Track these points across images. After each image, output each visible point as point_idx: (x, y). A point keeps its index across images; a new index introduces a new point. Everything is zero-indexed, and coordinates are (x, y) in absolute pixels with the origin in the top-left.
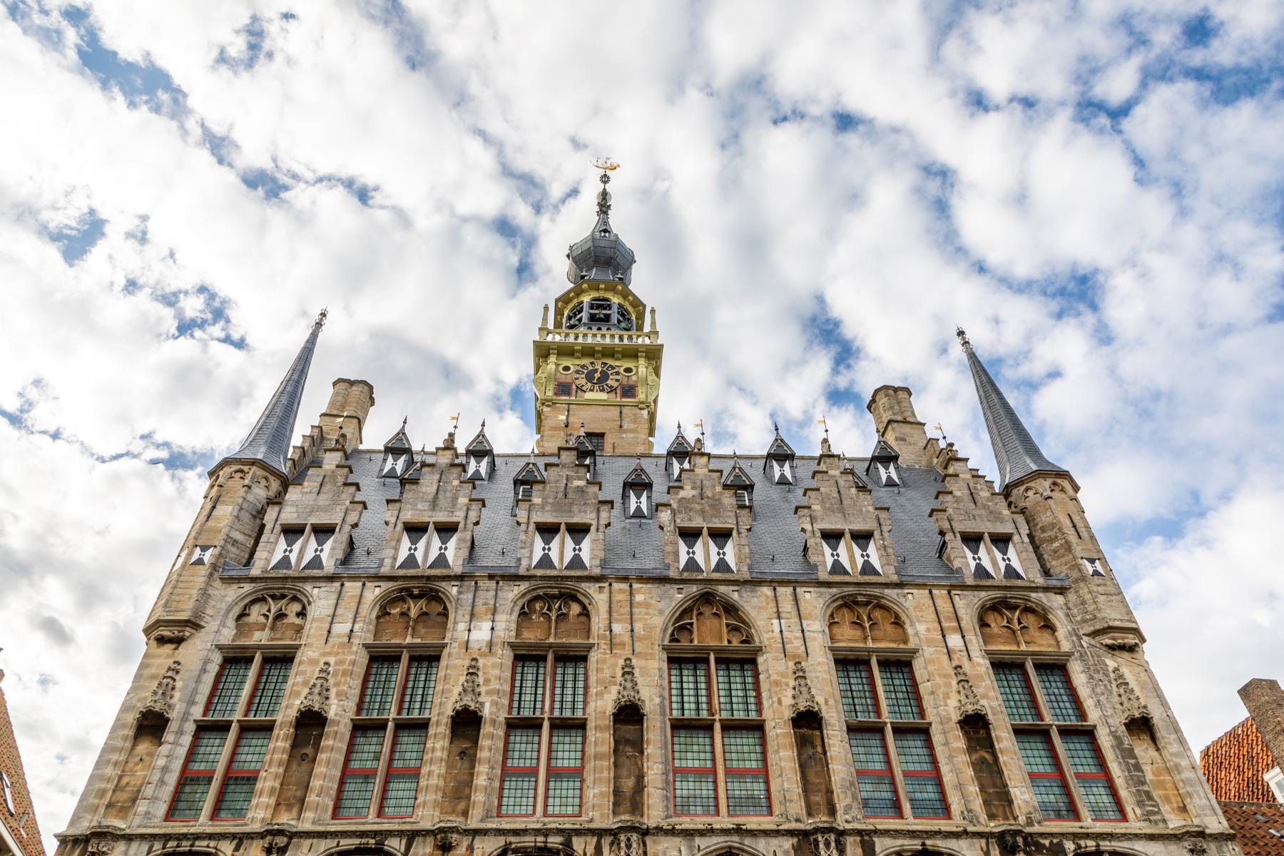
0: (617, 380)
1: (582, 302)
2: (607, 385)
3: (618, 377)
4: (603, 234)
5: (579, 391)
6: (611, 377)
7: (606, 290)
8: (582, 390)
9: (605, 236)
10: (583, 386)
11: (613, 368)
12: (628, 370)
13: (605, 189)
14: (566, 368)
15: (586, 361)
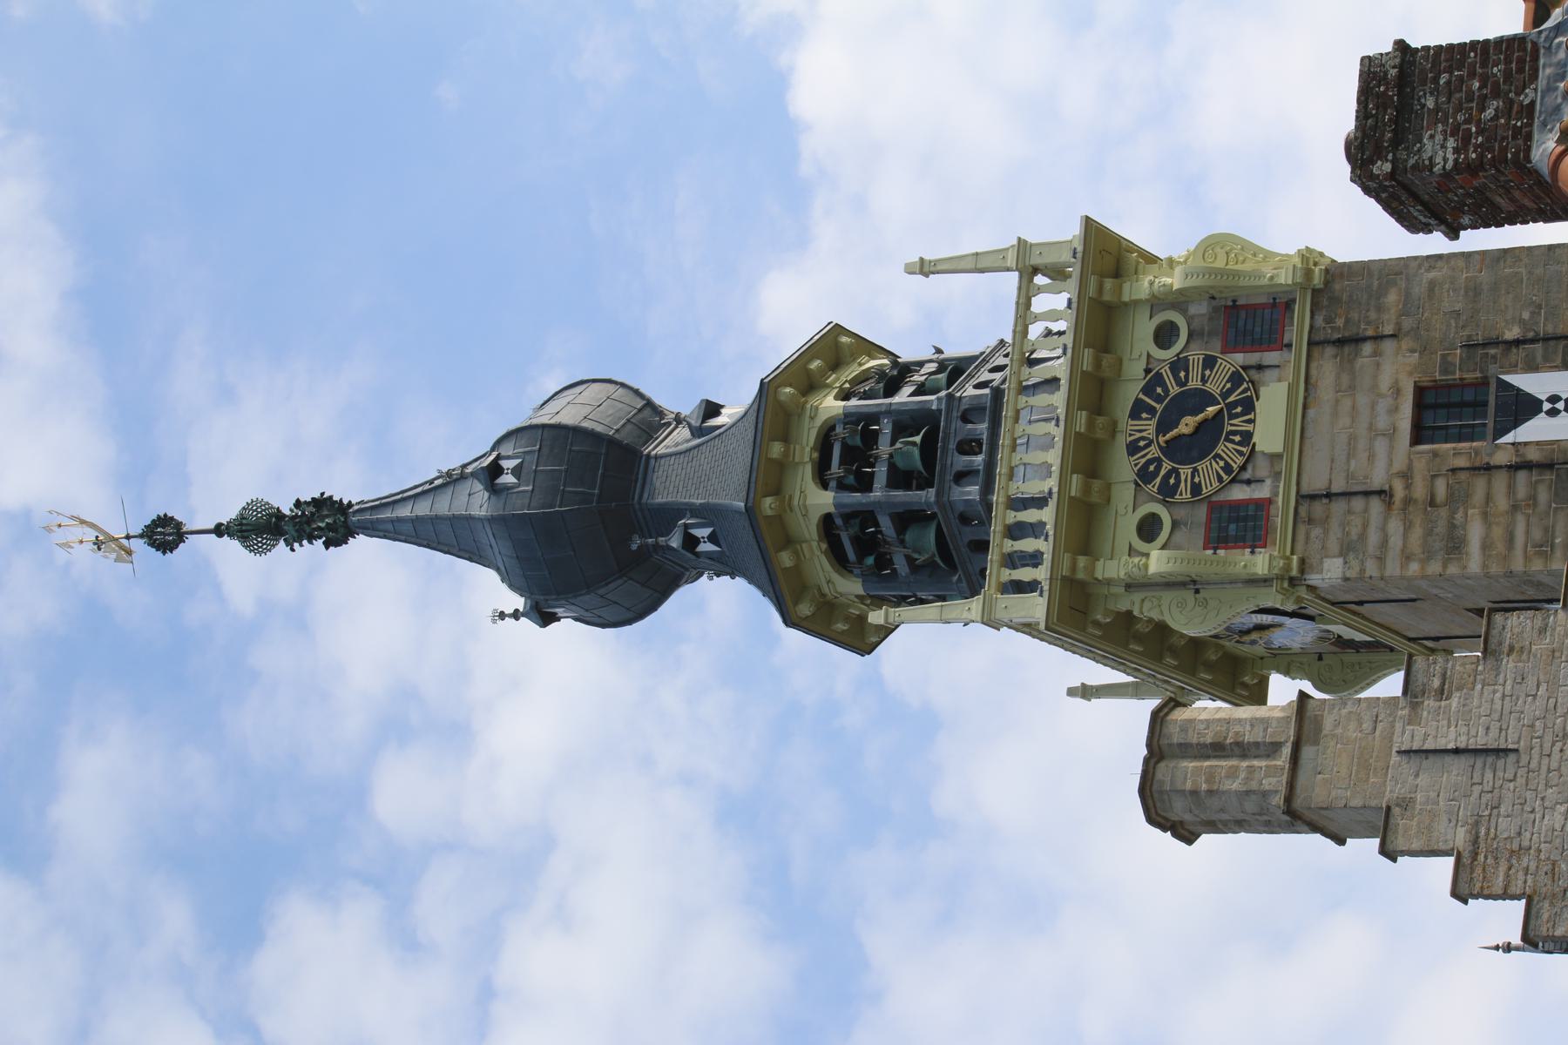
0: (1209, 362)
1: (827, 520)
2: (1225, 395)
3: (1196, 356)
4: (508, 479)
5: (1246, 475)
6: (1195, 383)
7: (786, 438)
8: (1243, 468)
9: (517, 471)
10: (1227, 468)
11: (1153, 383)
12: (1165, 335)
13: (219, 531)
14: (1149, 528)
15: (1123, 469)
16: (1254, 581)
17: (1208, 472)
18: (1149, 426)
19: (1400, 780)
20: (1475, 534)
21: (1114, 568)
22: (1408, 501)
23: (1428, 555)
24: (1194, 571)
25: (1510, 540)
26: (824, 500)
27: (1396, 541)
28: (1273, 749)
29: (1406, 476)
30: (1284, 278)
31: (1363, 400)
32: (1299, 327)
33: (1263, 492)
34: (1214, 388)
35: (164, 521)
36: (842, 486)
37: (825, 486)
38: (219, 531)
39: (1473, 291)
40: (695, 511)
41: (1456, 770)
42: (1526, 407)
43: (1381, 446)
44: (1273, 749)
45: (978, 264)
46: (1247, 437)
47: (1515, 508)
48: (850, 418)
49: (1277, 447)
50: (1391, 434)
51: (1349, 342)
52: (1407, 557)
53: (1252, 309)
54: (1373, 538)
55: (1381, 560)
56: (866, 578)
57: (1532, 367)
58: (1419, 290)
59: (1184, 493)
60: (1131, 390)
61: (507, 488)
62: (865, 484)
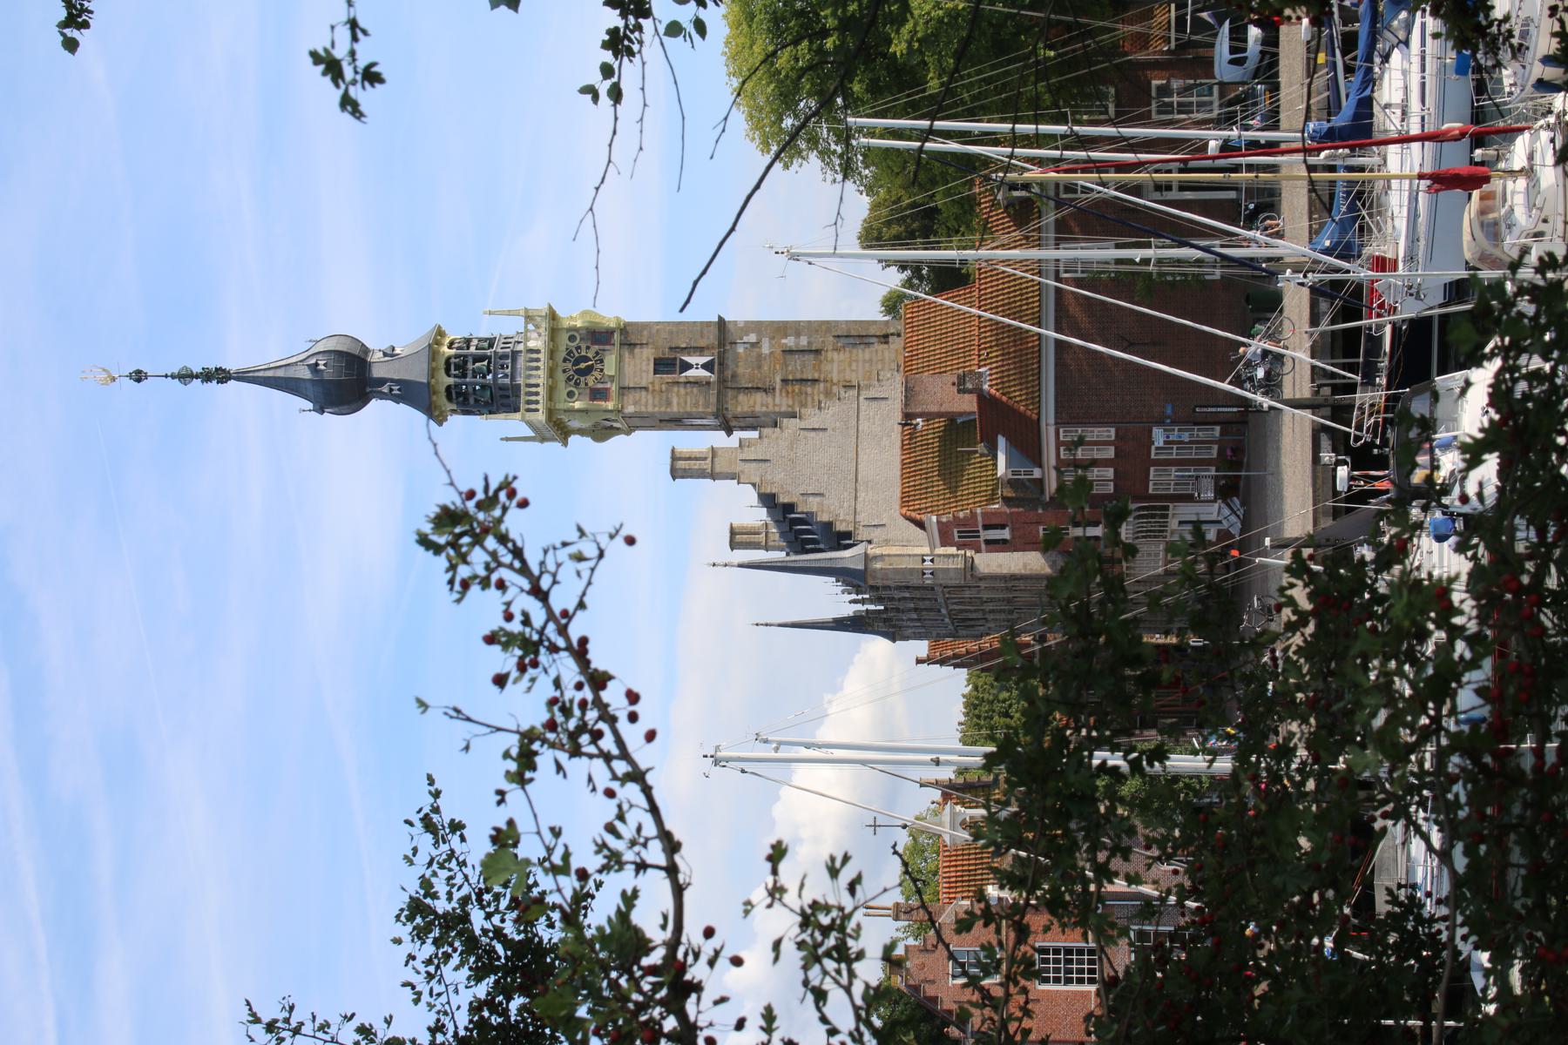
0: (588, 348)
1: (448, 388)
3: (583, 346)
11: (570, 353)
12: (572, 338)
14: (571, 394)
16: (607, 411)
17: (590, 380)
18: (569, 365)
19: (740, 467)
20: (675, 400)
21: (561, 406)
22: (654, 391)
23: (661, 405)
24: (589, 407)
25: (686, 403)
26: (451, 381)
27: (650, 401)
28: (705, 459)
29: (653, 383)
30: (612, 325)
31: (638, 361)
32: (616, 336)
33: (608, 386)
34: (590, 355)
35: (139, 372)
36: (455, 376)
37: (449, 375)
38: (166, 376)
39: (671, 333)
40: (392, 380)
41: (754, 465)
42: (688, 366)
43: (644, 375)
44: (705, 459)
45: (509, 313)
46: (602, 370)
47: (687, 394)
48: (456, 356)
49: (612, 373)
50: (647, 372)
51: (632, 345)
52: (654, 406)
53: (600, 333)
54: (644, 400)
55: (646, 406)
56: (457, 404)
57: (689, 355)
58: (654, 331)
59: (582, 385)
60: (562, 354)
61: (322, 371)
62: (464, 376)
